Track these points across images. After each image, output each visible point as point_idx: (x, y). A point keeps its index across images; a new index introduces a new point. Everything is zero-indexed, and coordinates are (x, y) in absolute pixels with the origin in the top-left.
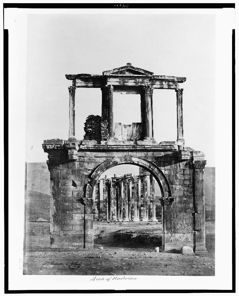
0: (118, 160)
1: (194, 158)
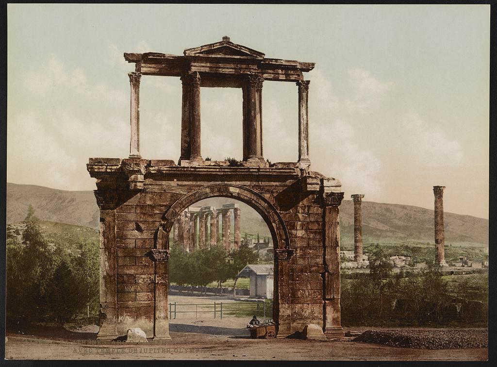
0: (208, 190)
1: (325, 188)
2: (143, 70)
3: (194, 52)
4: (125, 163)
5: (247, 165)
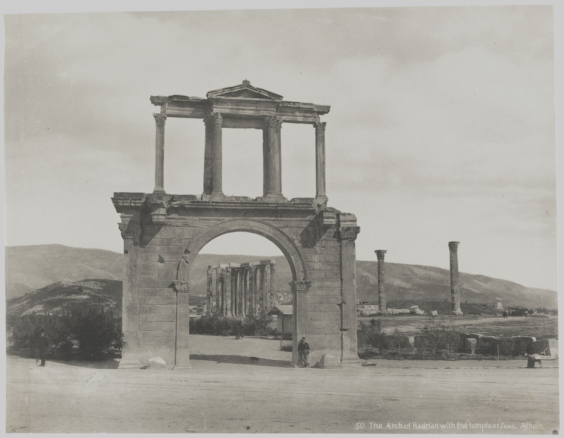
1: (342, 223)
2: (168, 112)
3: (215, 95)
4: (149, 196)
5: (267, 200)
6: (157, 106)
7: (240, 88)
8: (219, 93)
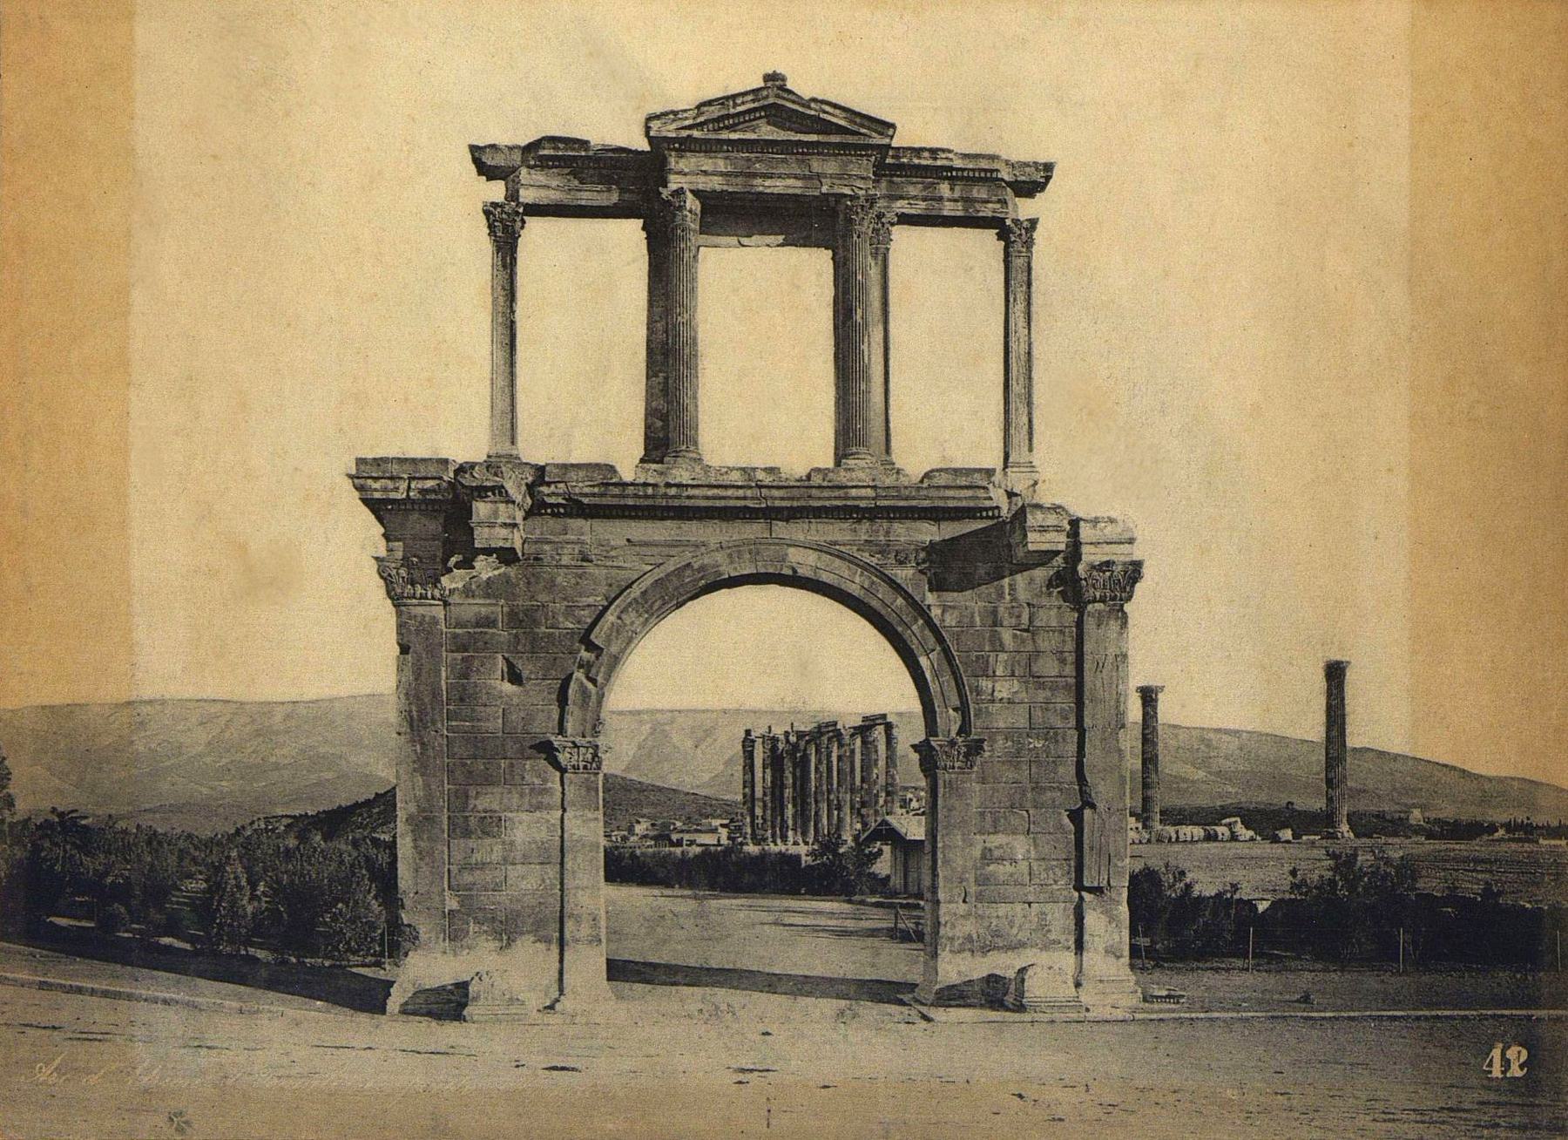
1: (1085, 549)
2: (527, 196)
3: (674, 126)
5: (842, 477)
6: (493, 182)
7: (753, 101)
8: (686, 118)
